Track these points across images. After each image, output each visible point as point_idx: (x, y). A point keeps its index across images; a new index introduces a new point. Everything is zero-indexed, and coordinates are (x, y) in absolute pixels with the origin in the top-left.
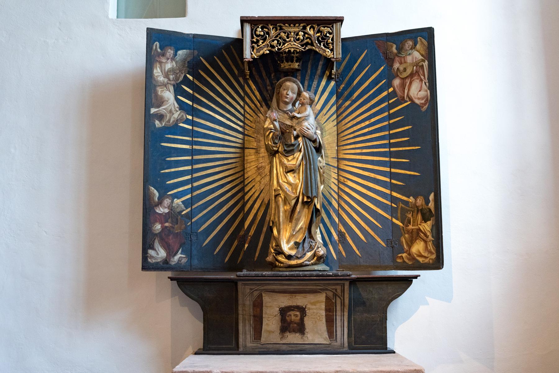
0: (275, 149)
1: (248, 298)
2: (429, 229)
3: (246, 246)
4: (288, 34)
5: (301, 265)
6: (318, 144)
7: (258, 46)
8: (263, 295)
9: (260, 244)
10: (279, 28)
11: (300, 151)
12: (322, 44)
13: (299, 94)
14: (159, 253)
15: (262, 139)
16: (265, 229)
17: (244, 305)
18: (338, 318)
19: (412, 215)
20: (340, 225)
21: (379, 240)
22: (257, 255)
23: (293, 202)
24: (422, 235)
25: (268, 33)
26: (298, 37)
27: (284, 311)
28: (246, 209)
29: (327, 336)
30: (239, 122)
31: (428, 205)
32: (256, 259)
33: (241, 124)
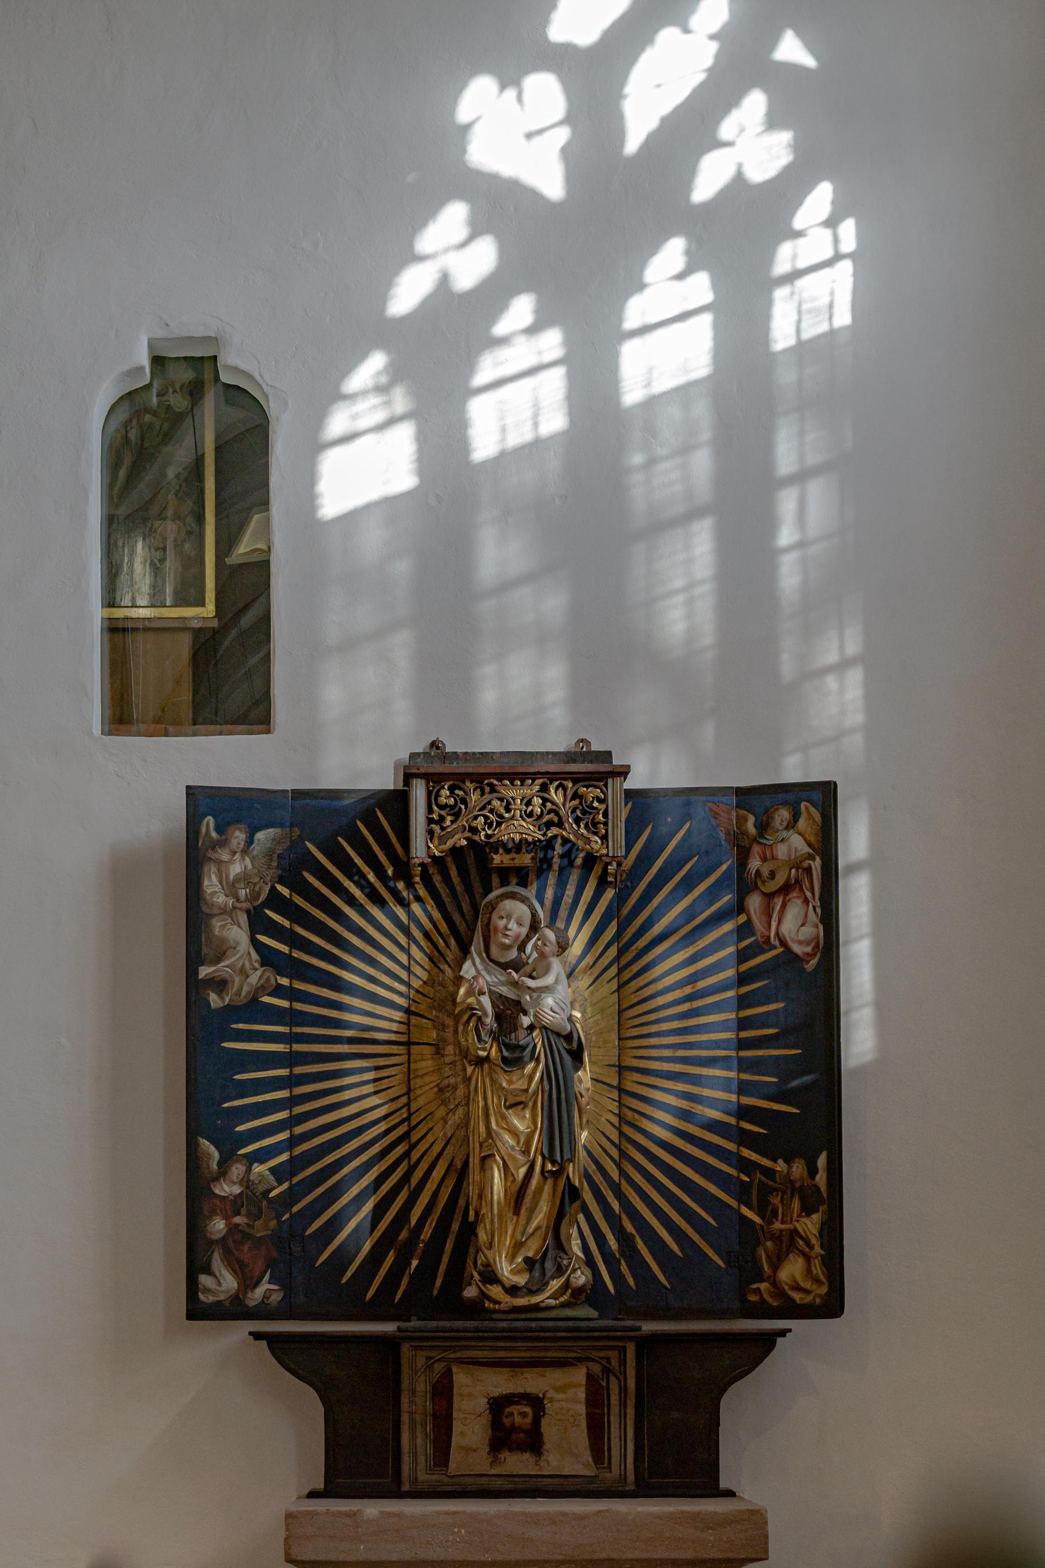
1: (423, 1378)
2: (815, 1231)
3: (415, 1263)
4: (508, 803)
5: (536, 1308)
6: (575, 1045)
7: (443, 829)
8: (454, 1369)
9: (445, 1260)
10: (487, 789)
11: (538, 1060)
12: (582, 826)
13: (534, 927)
14: (222, 1281)
15: (449, 1022)
16: (455, 1226)
17: (413, 1392)
18: (614, 1420)
19: (782, 1201)
20: (624, 1217)
21: (711, 1253)
22: (438, 1283)
24: (801, 1242)
25: (464, 801)
26: (530, 808)
27: (498, 1405)
28: (415, 1180)
29: (590, 1459)
30: (396, 985)
31: (813, 1178)
32: (435, 1293)
33: (403, 988)
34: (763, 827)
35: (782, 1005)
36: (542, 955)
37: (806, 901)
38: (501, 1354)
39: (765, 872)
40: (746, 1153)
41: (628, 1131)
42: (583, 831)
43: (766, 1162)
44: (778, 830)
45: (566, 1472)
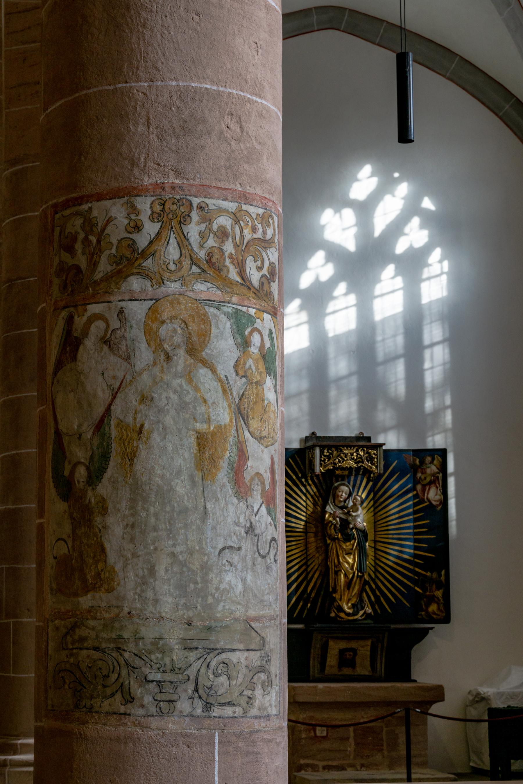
0: (336, 537)
2: (441, 595)
3: (309, 605)
7: (325, 463)
21: (405, 602)
23: (351, 575)
25: (332, 454)
27: (342, 652)
30: (302, 513)
33: (304, 514)
34: (422, 462)
35: (429, 521)
37: (437, 487)
38: (346, 635)
39: (423, 477)
40: (417, 569)
41: (378, 562)
42: (370, 464)
43: (423, 572)
44: (427, 464)
45: (362, 674)
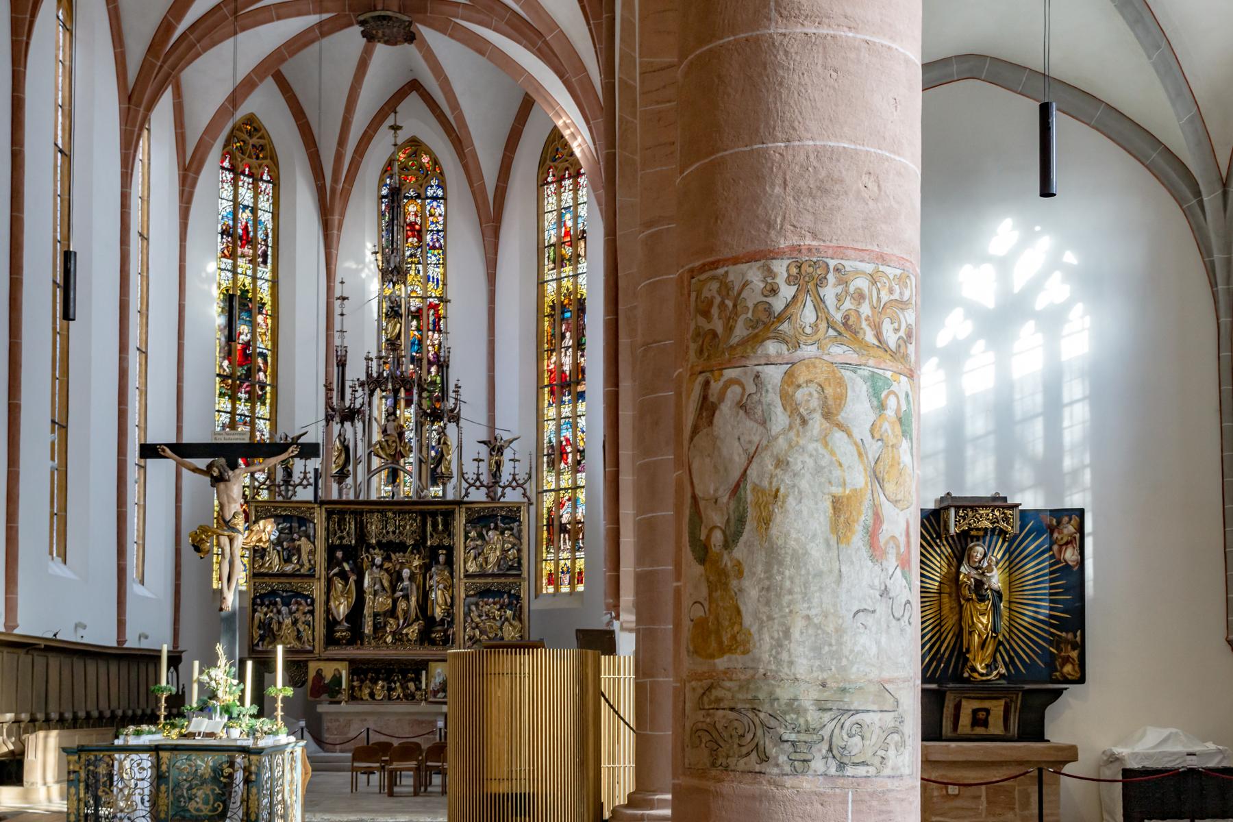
27: (975, 712)
34: (1059, 523)
36: (990, 565)
